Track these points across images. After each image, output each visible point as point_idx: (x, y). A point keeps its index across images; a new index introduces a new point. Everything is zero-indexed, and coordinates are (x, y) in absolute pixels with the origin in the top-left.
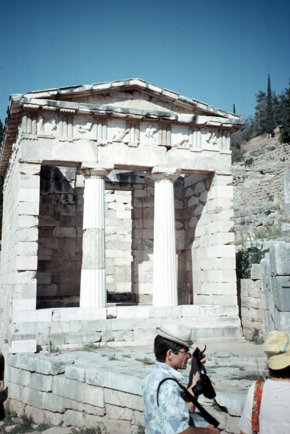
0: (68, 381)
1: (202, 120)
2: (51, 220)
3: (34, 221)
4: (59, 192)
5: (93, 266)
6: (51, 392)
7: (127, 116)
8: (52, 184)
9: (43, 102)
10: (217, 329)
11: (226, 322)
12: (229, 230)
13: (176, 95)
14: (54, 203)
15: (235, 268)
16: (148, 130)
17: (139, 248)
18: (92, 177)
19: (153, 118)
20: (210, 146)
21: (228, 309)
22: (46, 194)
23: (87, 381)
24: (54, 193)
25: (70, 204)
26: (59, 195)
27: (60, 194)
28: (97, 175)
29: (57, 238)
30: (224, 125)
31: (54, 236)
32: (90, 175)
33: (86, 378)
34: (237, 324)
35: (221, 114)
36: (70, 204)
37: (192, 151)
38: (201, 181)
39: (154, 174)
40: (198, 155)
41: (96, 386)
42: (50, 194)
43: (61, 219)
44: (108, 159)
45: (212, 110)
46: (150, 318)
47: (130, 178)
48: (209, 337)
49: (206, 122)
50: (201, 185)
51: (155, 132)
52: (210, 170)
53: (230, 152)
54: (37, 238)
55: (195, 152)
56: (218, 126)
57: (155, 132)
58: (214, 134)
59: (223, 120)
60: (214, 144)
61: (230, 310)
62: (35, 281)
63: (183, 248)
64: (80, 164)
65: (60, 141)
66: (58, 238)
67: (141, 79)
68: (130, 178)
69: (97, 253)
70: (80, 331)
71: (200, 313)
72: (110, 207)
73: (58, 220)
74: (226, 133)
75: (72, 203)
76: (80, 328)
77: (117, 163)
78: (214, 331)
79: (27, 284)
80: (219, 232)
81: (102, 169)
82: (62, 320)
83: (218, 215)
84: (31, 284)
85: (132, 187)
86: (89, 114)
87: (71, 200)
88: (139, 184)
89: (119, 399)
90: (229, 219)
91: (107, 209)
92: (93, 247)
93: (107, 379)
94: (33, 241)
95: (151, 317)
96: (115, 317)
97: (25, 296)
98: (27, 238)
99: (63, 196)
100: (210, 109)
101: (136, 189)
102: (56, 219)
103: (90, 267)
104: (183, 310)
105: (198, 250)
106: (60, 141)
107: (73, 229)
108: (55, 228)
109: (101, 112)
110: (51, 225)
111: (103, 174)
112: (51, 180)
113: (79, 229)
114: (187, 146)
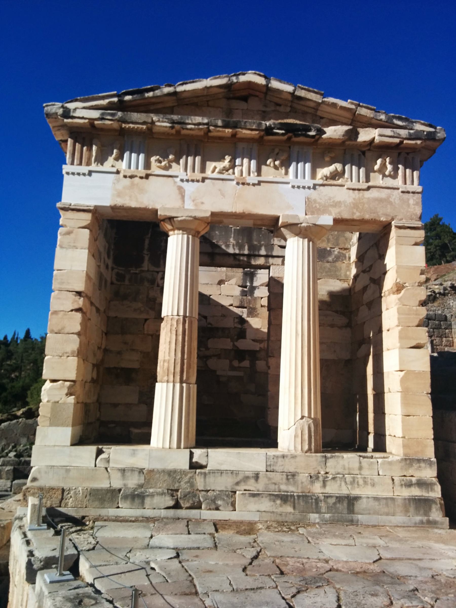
2: (142, 309)
3: (76, 301)
4: (156, 269)
8: (147, 258)
9: (95, 114)
10: (393, 499)
11: (413, 489)
12: (416, 323)
13: (319, 96)
14: (146, 284)
15: (429, 391)
21: (416, 465)
22: (137, 272)
24: (148, 271)
26: (156, 274)
29: (149, 335)
31: (146, 332)
34: (436, 493)
37: (349, 189)
38: (372, 246)
40: (361, 194)
42: (143, 271)
44: (202, 203)
46: (267, 471)
47: (263, 248)
48: (378, 514)
49: (374, 138)
50: (373, 253)
52: (382, 219)
53: (420, 189)
54: (78, 328)
55: (354, 190)
58: (388, 160)
59: (404, 133)
61: (420, 467)
62: (72, 399)
63: (348, 357)
64: (157, 211)
66: (152, 336)
67: (257, 72)
68: (263, 248)
69: (179, 355)
70: (141, 486)
71: (360, 468)
72: (262, 305)
74: (413, 158)
76: (142, 481)
77: (217, 209)
78: (387, 505)
79: (58, 402)
80: (398, 326)
81: (192, 219)
82: (111, 465)
84: (64, 403)
86: (172, 135)
90: (417, 303)
91: (260, 306)
94: (73, 333)
95: (269, 470)
96: (205, 467)
97: (55, 421)
98: (63, 328)
100: (380, 116)
101: (272, 264)
102: (150, 308)
103: (166, 378)
104: (327, 461)
108: (148, 321)
109: (189, 127)
110: (144, 316)
112: (145, 252)
114: (340, 181)
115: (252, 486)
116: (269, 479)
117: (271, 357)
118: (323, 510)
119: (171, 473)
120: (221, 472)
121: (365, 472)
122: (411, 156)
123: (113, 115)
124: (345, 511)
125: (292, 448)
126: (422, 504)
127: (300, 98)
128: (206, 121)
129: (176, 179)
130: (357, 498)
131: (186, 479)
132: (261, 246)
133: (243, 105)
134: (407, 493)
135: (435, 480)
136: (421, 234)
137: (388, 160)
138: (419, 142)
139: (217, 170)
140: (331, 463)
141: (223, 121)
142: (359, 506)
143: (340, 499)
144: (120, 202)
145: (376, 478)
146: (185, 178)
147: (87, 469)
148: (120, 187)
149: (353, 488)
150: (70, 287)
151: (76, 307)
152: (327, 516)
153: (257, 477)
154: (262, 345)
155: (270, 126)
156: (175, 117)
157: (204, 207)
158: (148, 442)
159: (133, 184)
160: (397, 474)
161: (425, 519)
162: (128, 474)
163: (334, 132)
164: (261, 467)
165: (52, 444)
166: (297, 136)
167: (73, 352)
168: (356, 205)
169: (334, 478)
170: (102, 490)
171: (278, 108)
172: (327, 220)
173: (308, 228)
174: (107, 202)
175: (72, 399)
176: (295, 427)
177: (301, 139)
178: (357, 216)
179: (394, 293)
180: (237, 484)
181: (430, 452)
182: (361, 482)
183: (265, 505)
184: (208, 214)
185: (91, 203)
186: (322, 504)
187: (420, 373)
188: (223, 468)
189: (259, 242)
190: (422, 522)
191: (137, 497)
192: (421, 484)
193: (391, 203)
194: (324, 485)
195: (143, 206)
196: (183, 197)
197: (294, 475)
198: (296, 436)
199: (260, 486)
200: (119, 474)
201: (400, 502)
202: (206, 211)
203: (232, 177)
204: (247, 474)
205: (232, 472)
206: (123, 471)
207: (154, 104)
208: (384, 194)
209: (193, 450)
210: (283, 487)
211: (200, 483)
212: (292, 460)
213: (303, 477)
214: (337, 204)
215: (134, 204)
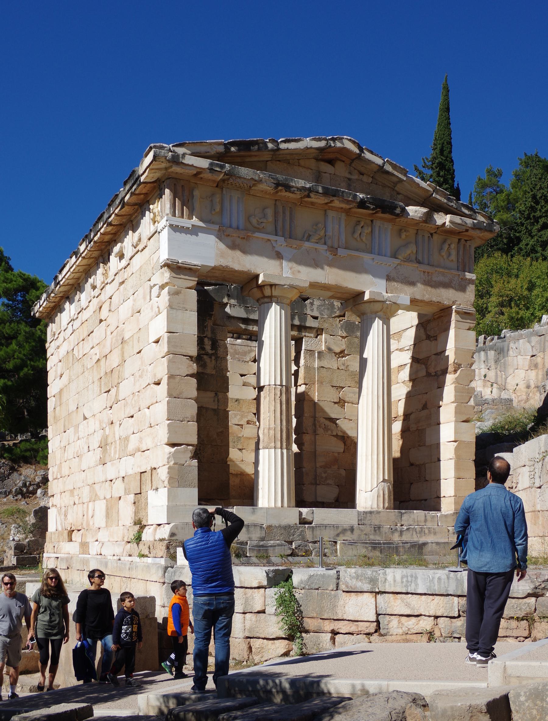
33: (341, 583)
41: (361, 592)
44: (299, 272)
89: (408, 605)
93: (386, 579)
117: (304, 433)
174: (212, 263)
187: (469, 443)
195: (246, 270)
215: (237, 267)
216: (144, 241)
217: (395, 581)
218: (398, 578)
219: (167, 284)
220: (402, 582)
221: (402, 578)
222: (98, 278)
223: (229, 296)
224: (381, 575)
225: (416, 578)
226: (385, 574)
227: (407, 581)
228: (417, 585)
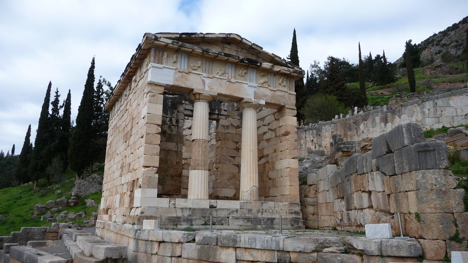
0: (199, 247)
1: (277, 68)
4: (166, 116)
5: (200, 168)
6: (180, 256)
7: (228, 59)
10: (286, 219)
16: (241, 71)
17: (222, 162)
18: (201, 100)
19: (245, 62)
20: (281, 88)
21: (293, 206)
23: (219, 244)
25: (173, 125)
27: (167, 117)
28: (204, 99)
30: (292, 74)
32: (199, 99)
34: (300, 216)
35: (290, 66)
36: (173, 125)
39: (244, 103)
43: (167, 135)
45: (284, 62)
51: (245, 73)
53: (295, 93)
56: (287, 74)
57: (245, 73)
59: (291, 70)
60: (284, 86)
62: (157, 175)
65: (179, 72)
70: (190, 216)
71: (275, 207)
73: (165, 137)
75: (175, 124)
76: (190, 213)
83: (287, 137)
84: (154, 177)
85: (218, 117)
87: (174, 122)
88: (223, 115)
89: (252, 255)
92: (200, 153)
93: (240, 240)
96: (216, 207)
97: (149, 186)
98: (152, 142)
99: (168, 119)
105: (267, 165)
106: (179, 72)
107: (175, 144)
109: (210, 54)
111: (208, 99)
113: (179, 145)
115: (235, 215)
116: (242, 212)
118: (262, 224)
119: (203, 210)
120: (223, 209)
121: (276, 209)
122: (291, 79)
123: (177, 43)
124: (270, 224)
125: (249, 199)
126: (296, 221)
127: (254, 48)
128: (217, 52)
129: (202, 76)
130: (274, 219)
131: (209, 212)
132: (216, 109)
133: (228, 46)
134: (290, 216)
135: (300, 211)
136: (295, 112)
137: (284, 80)
138: (296, 74)
139: (219, 74)
140: (264, 205)
141: (224, 53)
142: (276, 221)
143: (268, 219)
144: (177, 83)
145: (281, 211)
146: (206, 76)
147: (167, 208)
148: (177, 76)
149: (272, 215)
150: (155, 122)
151: (158, 132)
152: (264, 226)
153: (237, 211)
154: (186, 161)
155: (243, 59)
156: (205, 48)
157: (214, 90)
158: (185, 196)
159: (182, 76)
160: (287, 209)
161: (297, 226)
162: (184, 210)
163: (266, 65)
164: (238, 207)
165: (149, 196)
166: (252, 64)
167: (157, 153)
168: (273, 97)
169: (265, 211)
170: (173, 217)
171: (243, 50)
172: (263, 102)
173: (255, 105)
174: (171, 83)
175: (157, 175)
176: (249, 191)
177: (254, 66)
178: (273, 102)
179: (285, 136)
180: (229, 214)
181: (298, 201)
182: (275, 212)
183: (241, 222)
184: (216, 94)
185: (165, 82)
186: (262, 221)
188: (223, 207)
189: (215, 107)
190: (296, 227)
191: (189, 220)
192: (296, 213)
193: (285, 98)
194: (262, 214)
196: (204, 85)
197: (251, 210)
198: (251, 194)
199: (238, 215)
200: (181, 210)
201: (289, 220)
202: (215, 92)
203: (225, 78)
204: (233, 210)
205: (227, 209)
206: (182, 209)
207: (192, 40)
208: (282, 94)
209: (211, 200)
210: (247, 215)
211: (214, 214)
212: (250, 204)
213: (254, 211)
214: (266, 96)
215: (183, 86)
216: (143, 74)
217: (245, 241)
218: (247, 239)
219: (149, 92)
220: (249, 242)
221: (249, 240)
222: (126, 92)
223: (185, 100)
224: (238, 238)
225: (256, 240)
226: (240, 237)
227: (251, 242)
228: (256, 244)
